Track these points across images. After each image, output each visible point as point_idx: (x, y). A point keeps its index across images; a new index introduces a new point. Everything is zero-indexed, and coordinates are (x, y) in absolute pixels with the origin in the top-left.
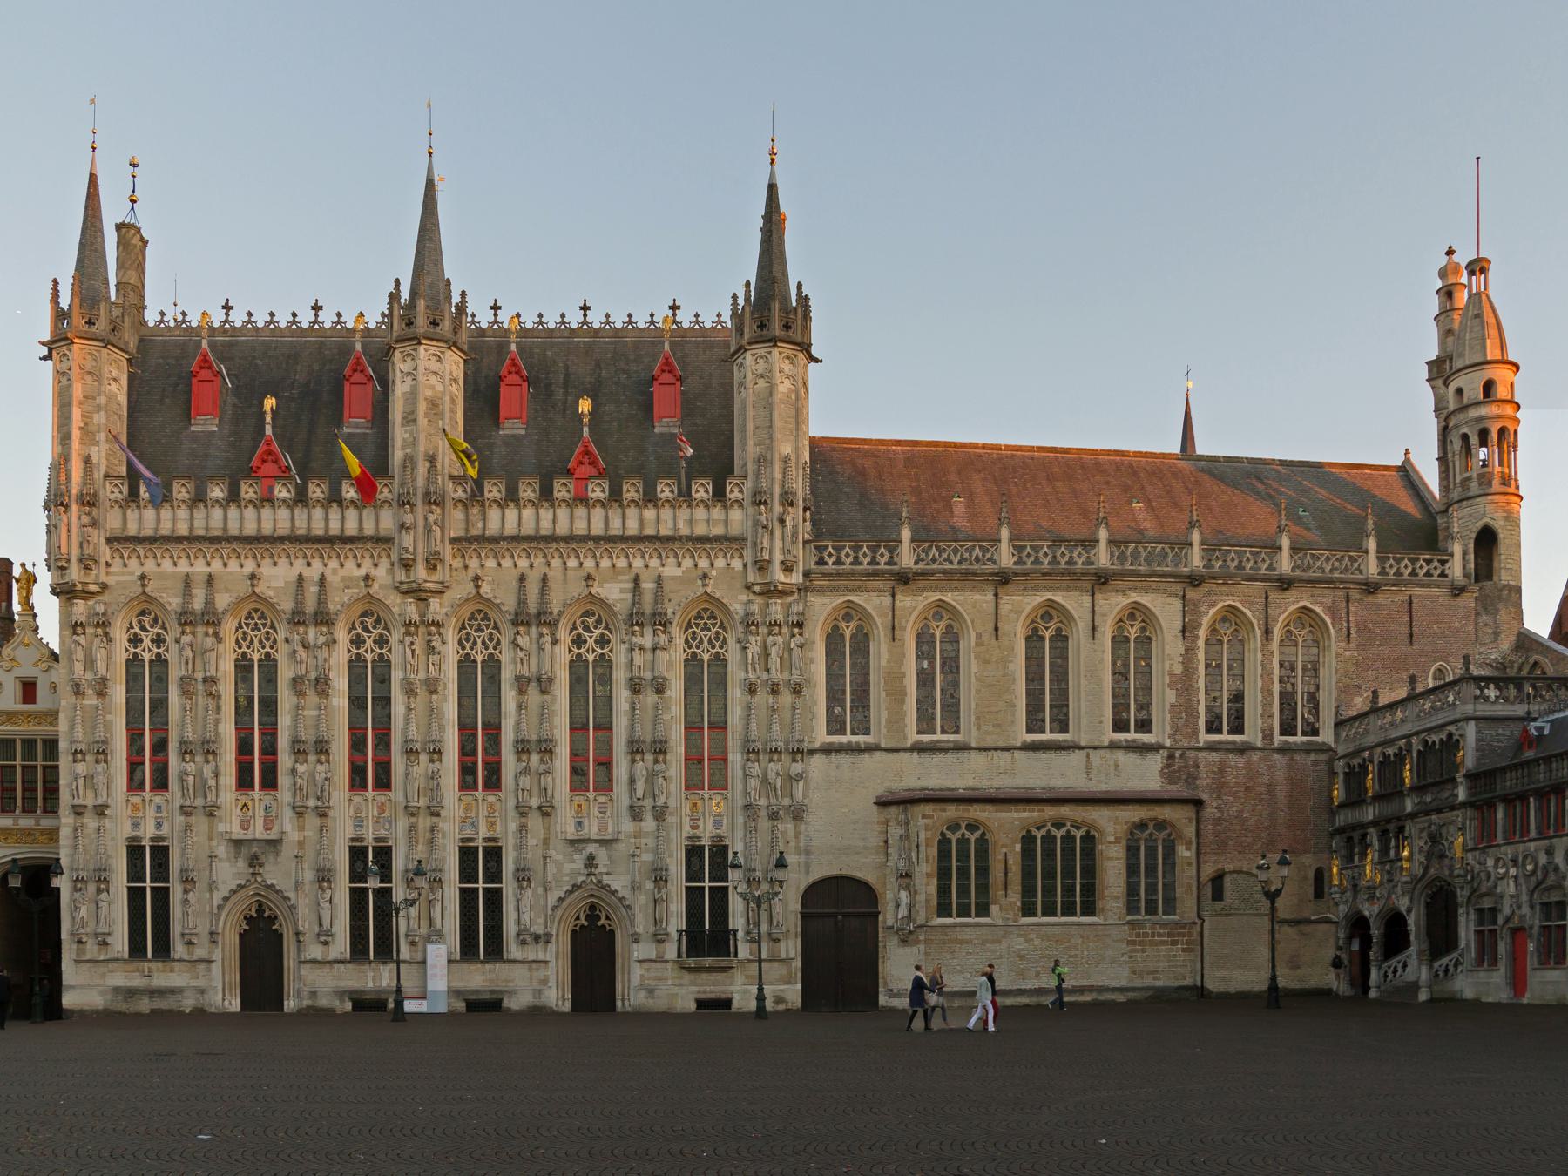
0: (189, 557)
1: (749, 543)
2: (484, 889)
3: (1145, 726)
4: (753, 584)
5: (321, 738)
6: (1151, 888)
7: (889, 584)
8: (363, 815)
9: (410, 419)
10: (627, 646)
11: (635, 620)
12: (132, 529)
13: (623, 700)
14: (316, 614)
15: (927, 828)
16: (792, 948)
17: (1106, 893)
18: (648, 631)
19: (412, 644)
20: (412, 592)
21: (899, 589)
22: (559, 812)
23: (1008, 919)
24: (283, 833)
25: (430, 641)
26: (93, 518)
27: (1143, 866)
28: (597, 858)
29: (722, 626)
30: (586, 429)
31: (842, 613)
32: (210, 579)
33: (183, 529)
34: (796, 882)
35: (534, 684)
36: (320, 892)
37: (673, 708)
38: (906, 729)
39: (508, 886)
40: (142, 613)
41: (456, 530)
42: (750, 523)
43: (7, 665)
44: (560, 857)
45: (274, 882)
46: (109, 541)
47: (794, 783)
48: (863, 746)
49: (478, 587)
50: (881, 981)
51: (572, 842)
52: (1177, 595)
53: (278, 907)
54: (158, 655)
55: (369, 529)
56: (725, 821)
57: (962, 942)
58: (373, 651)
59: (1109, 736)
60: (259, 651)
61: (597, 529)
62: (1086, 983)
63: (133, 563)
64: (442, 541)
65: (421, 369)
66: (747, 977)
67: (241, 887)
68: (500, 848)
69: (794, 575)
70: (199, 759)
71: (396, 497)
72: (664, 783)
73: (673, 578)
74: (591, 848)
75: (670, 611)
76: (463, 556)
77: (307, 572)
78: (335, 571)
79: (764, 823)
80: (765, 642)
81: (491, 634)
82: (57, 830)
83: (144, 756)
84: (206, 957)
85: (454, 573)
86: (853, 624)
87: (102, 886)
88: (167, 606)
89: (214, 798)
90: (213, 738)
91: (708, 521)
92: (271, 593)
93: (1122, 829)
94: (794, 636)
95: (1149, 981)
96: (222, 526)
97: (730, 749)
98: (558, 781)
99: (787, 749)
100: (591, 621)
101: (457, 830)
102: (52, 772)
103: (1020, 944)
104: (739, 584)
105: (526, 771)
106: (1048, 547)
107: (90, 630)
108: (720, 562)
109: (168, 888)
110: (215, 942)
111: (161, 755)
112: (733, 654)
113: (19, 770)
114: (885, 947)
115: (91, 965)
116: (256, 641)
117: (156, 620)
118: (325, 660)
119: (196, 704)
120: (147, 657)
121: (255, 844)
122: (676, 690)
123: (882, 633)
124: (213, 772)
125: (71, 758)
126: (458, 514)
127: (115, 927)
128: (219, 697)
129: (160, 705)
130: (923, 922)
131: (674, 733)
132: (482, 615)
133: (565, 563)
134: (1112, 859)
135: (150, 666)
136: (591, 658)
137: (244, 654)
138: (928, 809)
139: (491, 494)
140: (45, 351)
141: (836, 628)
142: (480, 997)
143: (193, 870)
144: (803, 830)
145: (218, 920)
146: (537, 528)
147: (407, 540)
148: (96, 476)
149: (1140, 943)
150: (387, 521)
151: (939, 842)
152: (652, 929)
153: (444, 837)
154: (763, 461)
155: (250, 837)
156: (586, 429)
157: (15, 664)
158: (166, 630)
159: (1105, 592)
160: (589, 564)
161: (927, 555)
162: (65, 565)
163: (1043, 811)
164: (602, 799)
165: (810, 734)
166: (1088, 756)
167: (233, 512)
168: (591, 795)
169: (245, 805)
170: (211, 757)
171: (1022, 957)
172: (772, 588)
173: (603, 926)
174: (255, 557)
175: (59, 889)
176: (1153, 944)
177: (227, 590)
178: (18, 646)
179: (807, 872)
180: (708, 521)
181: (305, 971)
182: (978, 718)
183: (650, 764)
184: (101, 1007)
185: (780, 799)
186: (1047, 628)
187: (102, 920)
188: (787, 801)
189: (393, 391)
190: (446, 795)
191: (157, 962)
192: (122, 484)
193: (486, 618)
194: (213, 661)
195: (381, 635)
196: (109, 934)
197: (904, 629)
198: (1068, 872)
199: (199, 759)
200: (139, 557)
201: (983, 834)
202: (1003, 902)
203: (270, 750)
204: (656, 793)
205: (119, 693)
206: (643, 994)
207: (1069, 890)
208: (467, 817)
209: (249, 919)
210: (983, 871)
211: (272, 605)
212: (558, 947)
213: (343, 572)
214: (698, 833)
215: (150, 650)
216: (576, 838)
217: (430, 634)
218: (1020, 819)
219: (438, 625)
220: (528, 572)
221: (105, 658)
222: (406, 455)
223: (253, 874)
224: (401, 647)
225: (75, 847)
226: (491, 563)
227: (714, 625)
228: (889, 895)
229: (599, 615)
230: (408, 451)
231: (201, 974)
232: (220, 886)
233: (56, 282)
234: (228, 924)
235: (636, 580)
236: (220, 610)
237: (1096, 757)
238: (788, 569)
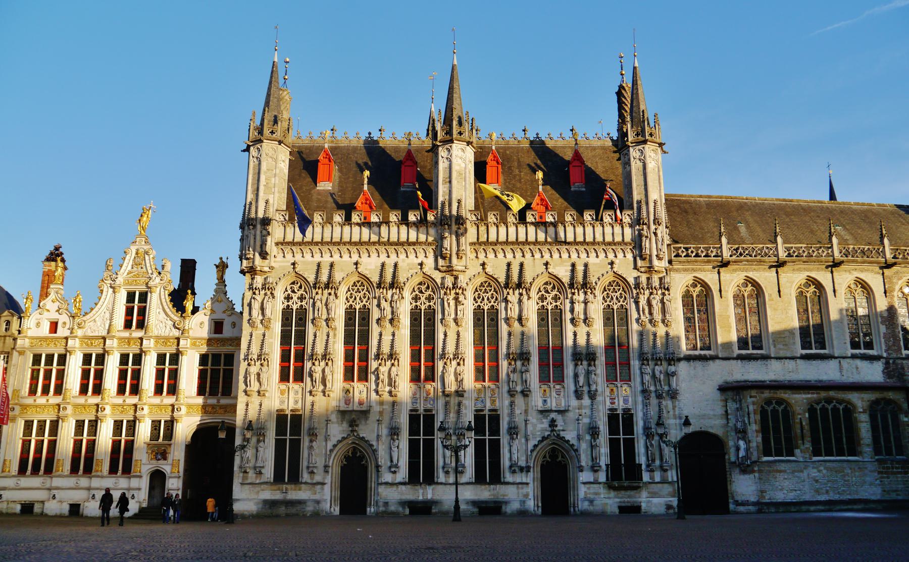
2: (489, 439)
3: (869, 346)
6: (887, 440)
15: (754, 404)
16: (672, 475)
17: (862, 442)
20: (448, 271)
21: (722, 270)
22: (533, 394)
23: (806, 458)
24: (370, 406)
27: (880, 426)
28: (557, 421)
32: (332, 265)
34: (675, 434)
36: (392, 441)
38: (733, 347)
39: (504, 439)
40: (293, 283)
44: (534, 421)
45: (364, 435)
46: (277, 244)
50: (730, 495)
51: (541, 412)
52: (879, 273)
56: (630, 400)
57: (780, 471)
58: (424, 303)
59: (850, 352)
62: (856, 497)
63: (289, 256)
66: (649, 493)
67: (344, 438)
68: (499, 415)
71: (439, 220)
74: (553, 415)
77: (388, 261)
78: (403, 260)
84: (322, 481)
85: (472, 261)
89: (331, 387)
92: (368, 272)
93: (866, 404)
95: (893, 496)
97: (631, 358)
98: (532, 376)
100: (549, 287)
101: (473, 405)
103: (815, 473)
105: (514, 371)
106: (805, 247)
109: (300, 439)
110: (327, 472)
115: (251, 486)
116: (358, 298)
117: (301, 287)
119: (322, 333)
120: (295, 307)
121: (354, 413)
127: (267, 463)
128: (335, 329)
130: (756, 459)
134: (862, 422)
136: (550, 307)
137: (351, 306)
138: (753, 393)
140: (245, 147)
141: (688, 291)
142: (488, 505)
144: (677, 405)
145: (329, 459)
149: (886, 473)
151: (761, 411)
152: (590, 463)
153: (466, 408)
155: (350, 409)
159: (839, 271)
161: (737, 252)
163: (819, 393)
164: (558, 387)
166: (840, 362)
167: (347, 229)
171: (817, 481)
173: (560, 461)
176: (893, 473)
177: (342, 270)
181: (382, 490)
182: (774, 341)
184: (255, 513)
185: (663, 387)
186: (808, 292)
187: (260, 459)
188: (666, 388)
191: (291, 484)
195: (430, 295)
196: (263, 467)
197: (727, 291)
198: (838, 429)
201: (786, 407)
202: (802, 447)
204: (591, 383)
205: (277, 327)
206: (586, 503)
207: (839, 441)
208: (478, 398)
209: (347, 458)
210: (788, 428)
212: (534, 475)
214: (615, 406)
215: (296, 303)
217: (457, 294)
218: (807, 399)
221: (271, 307)
223: (352, 431)
226: (491, 255)
228: (731, 443)
231: (318, 491)
232: (332, 438)
234: (335, 461)
235: (573, 265)
237: (845, 363)
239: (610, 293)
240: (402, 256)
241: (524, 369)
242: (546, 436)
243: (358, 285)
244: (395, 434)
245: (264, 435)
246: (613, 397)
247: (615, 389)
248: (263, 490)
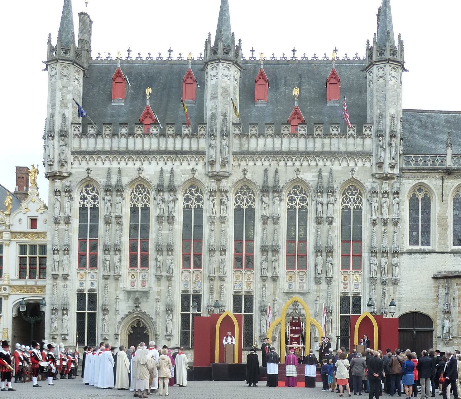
0: (109, 160)
1: (374, 155)
2: (244, 315)
4: (375, 174)
5: (170, 244)
7: (441, 175)
8: (188, 280)
9: (214, 97)
10: (315, 202)
11: (319, 191)
12: (84, 148)
13: (312, 227)
14: (169, 186)
18: (325, 195)
19: (213, 200)
24: (150, 288)
25: (222, 199)
26: (65, 142)
29: (360, 194)
30: (296, 102)
31: (418, 187)
32: (120, 171)
33: (107, 148)
35: (270, 219)
36: (167, 315)
37: (336, 231)
41: (235, 148)
42: (374, 145)
43: (24, 211)
44: (281, 301)
45: (146, 311)
46: (73, 153)
47: (394, 268)
48: (427, 251)
49: (245, 174)
51: (287, 294)
53: (147, 323)
54: (94, 205)
55: (194, 147)
60: (141, 203)
61: (302, 147)
64: (228, 153)
65: (220, 74)
68: (253, 296)
69: (395, 169)
70: (112, 253)
71: (207, 133)
72: (331, 266)
73: (337, 171)
74: (297, 297)
75: (335, 186)
76: (238, 160)
77: (165, 168)
79: (379, 287)
80: (381, 201)
81: (250, 196)
82: (45, 287)
83: (86, 252)
85: (234, 168)
86: (422, 193)
87: (65, 312)
88: (100, 183)
89: (119, 272)
90: (119, 244)
91: (354, 144)
92: (148, 177)
94: (395, 198)
96: (126, 146)
98: (280, 265)
99: (390, 251)
100: (298, 191)
101: (232, 288)
102: (43, 260)
104: (369, 174)
107: (63, 194)
108: (360, 164)
109: (95, 313)
110: (117, 339)
111: (94, 252)
112: (365, 207)
113: (28, 259)
114: (436, 346)
116: (140, 199)
117: (93, 189)
118: (173, 208)
119: (112, 228)
120: (89, 206)
122: (338, 223)
123: (437, 197)
124: (118, 259)
125: (52, 252)
126: (236, 141)
127: (70, 332)
128: (122, 225)
129: (94, 229)
131: (336, 243)
132: (246, 187)
133: (286, 164)
136: (297, 207)
139: (252, 132)
141: (414, 195)
143: (108, 305)
145: (118, 328)
146: (274, 148)
147: (212, 152)
148: (67, 123)
150: (203, 144)
153: (226, 290)
154: (381, 116)
156: (296, 102)
157: (27, 210)
158: (98, 194)
160: (298, 164)
162: (52, 163)
164: (301, 274)
165: (401, 244)
167: (131, 140)
168: (296, 271)
169: (133, 274)
170: (117, 252)
172: (385, 176)
174: (140, 160)
175: (44, 313)
177: (127, 175)
178: (30, 201)
179: (399, 310)
180: (354, 144)
183: (325, 258)
185: (387, 275)
188: (390, 276)
189: (206, 84)
190: (227, 271)
192: (79, 127)
193: (248, 189)
194: (120, 208)
195: (199, 196)
196: (67, 335)
197: (448, 196)
199: (112, 253)
200: (86, 160)
203: (145, 250)
204: (328, 271)
205: (75, 223)
209: (133, 328)
211: (148, 182)
214: (347, 290)
215: (90, 203)
216: (289, 292)
217: (222, 196)
219: (226, 192)
220: (269, 168)
222: (212, 113)
224: (208, 202)
225: (53, 294)
226: (251, 163)
227: (356, 193)
228: (439, 322)
229: (302, 187)
230: (214, 111)
232: (120, 313)
233: (50, 34)
235: (320, 172)
236: (124, 185)
238: (392, 167)
239: (349, 196)
240: (177, 163)
241: (274, 258)
242: (290, 313)
243: (140, 188)
244: (169, 310)
246: (346, 282)
247: (348, 276)
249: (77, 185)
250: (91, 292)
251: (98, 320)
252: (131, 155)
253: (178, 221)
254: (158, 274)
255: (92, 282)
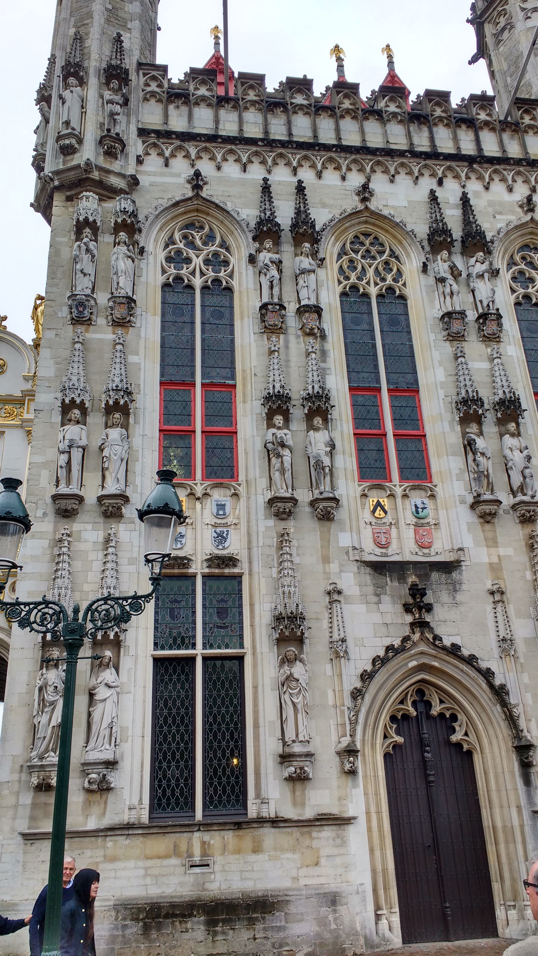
32: (300, 189)
45: (457, 641)
46: (143, 133)
54: (217, 281)
84: (335, 810)
88: (235, 215)
116: (371, 272)
119: (287, 347)
120: (198, 282)
125: (57, 418)
127: (126, 747)
128: (323, 337)
135: (202, 294)
145: (354, 723)
158: (228, 249)
169: (379, 504)
177: (324, 206)
191: (223, 826)
196: (111, 764)
213: (487, 196)
215: (202, 274)
231: (324, 852)
243: (367, 242)
245: (117, 644)
248: (113, 859)
249: (157, 216)
250: (218, 566)
251: (255, 687)
252: (333, 155)
253: (510, 333)
254: (488, 496)
255: (218, 530)
